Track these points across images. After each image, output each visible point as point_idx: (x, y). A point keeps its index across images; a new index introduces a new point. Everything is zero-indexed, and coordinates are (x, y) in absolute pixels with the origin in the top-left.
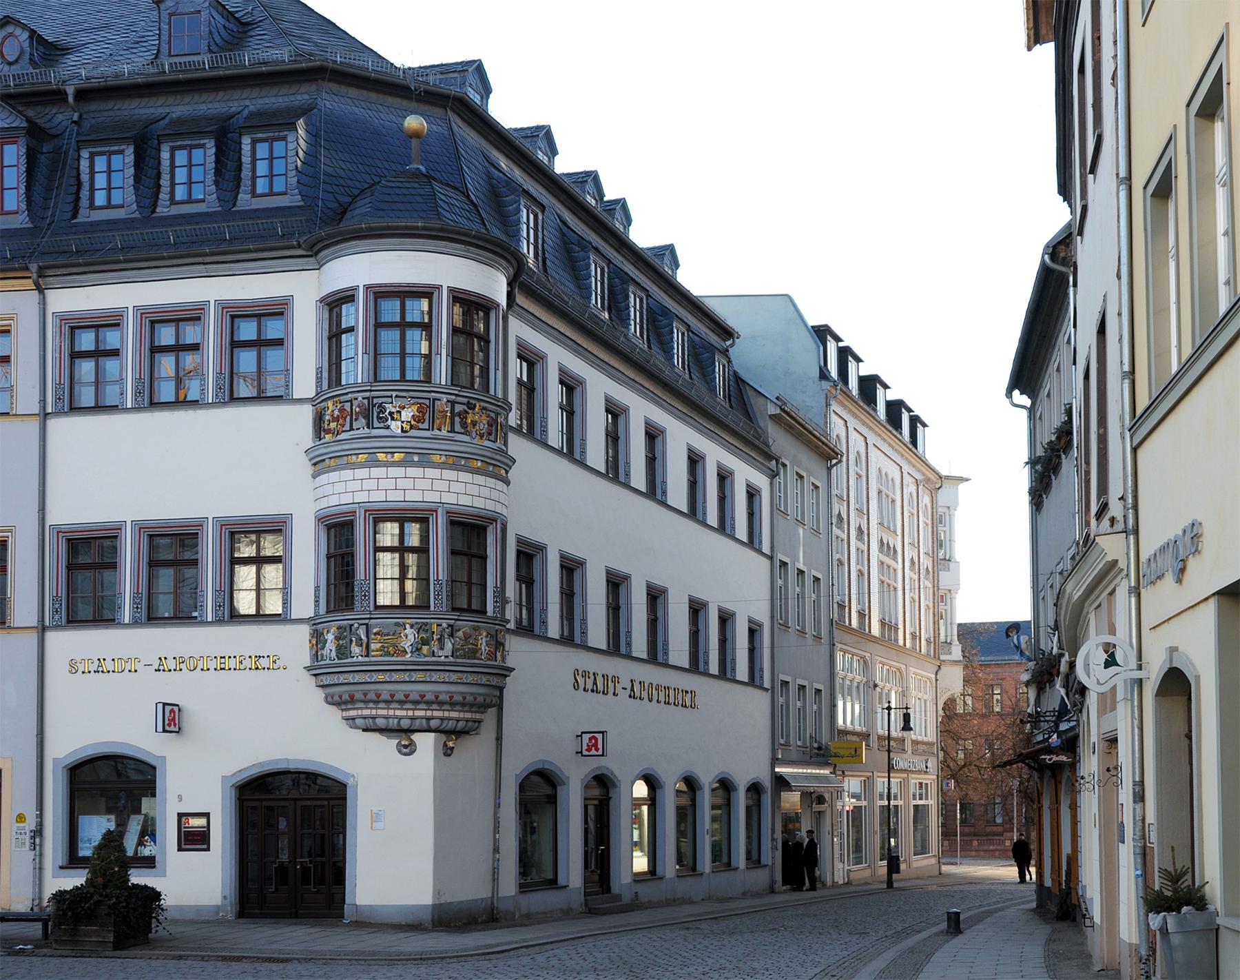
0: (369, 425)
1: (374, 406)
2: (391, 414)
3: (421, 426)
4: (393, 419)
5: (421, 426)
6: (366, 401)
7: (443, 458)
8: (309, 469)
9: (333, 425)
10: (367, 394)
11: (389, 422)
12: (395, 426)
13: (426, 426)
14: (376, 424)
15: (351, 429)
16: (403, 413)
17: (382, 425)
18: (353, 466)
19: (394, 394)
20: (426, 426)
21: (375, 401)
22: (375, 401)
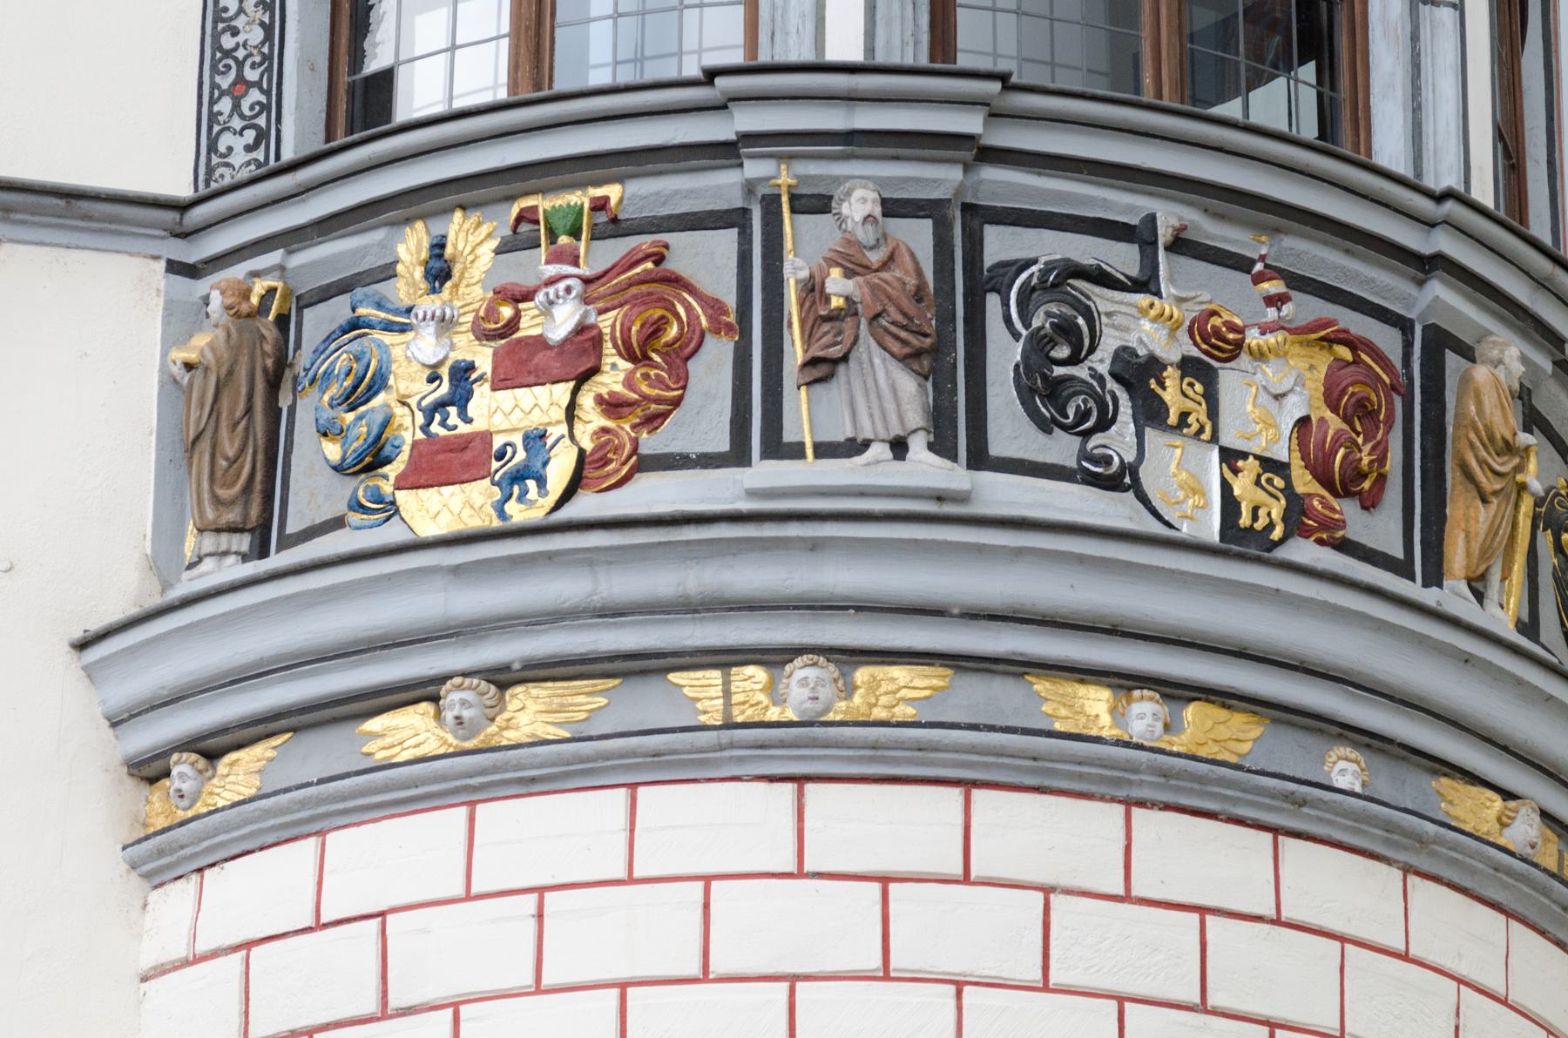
0: (958, 429)
1: (983, 281)
2: (1138, 373)
3: (1357, 523)
4: (1151, 413)
5: (1357, 523)
6: (918, 235)
7: (1524, 830)
8: (89, 809)
9: (499, 412)
10: (940, 178)
11: (1120, 440)
12: (1186, 482)
13: (1382, 528)
14: (1010, 428)
15: (757, 431)
16: (1230, 380)
17: (1062, 449)
18: (798, 757)
19: (1169, 215)
20: (1382, 528)
21: (999, 244)
22: (999, 244)
